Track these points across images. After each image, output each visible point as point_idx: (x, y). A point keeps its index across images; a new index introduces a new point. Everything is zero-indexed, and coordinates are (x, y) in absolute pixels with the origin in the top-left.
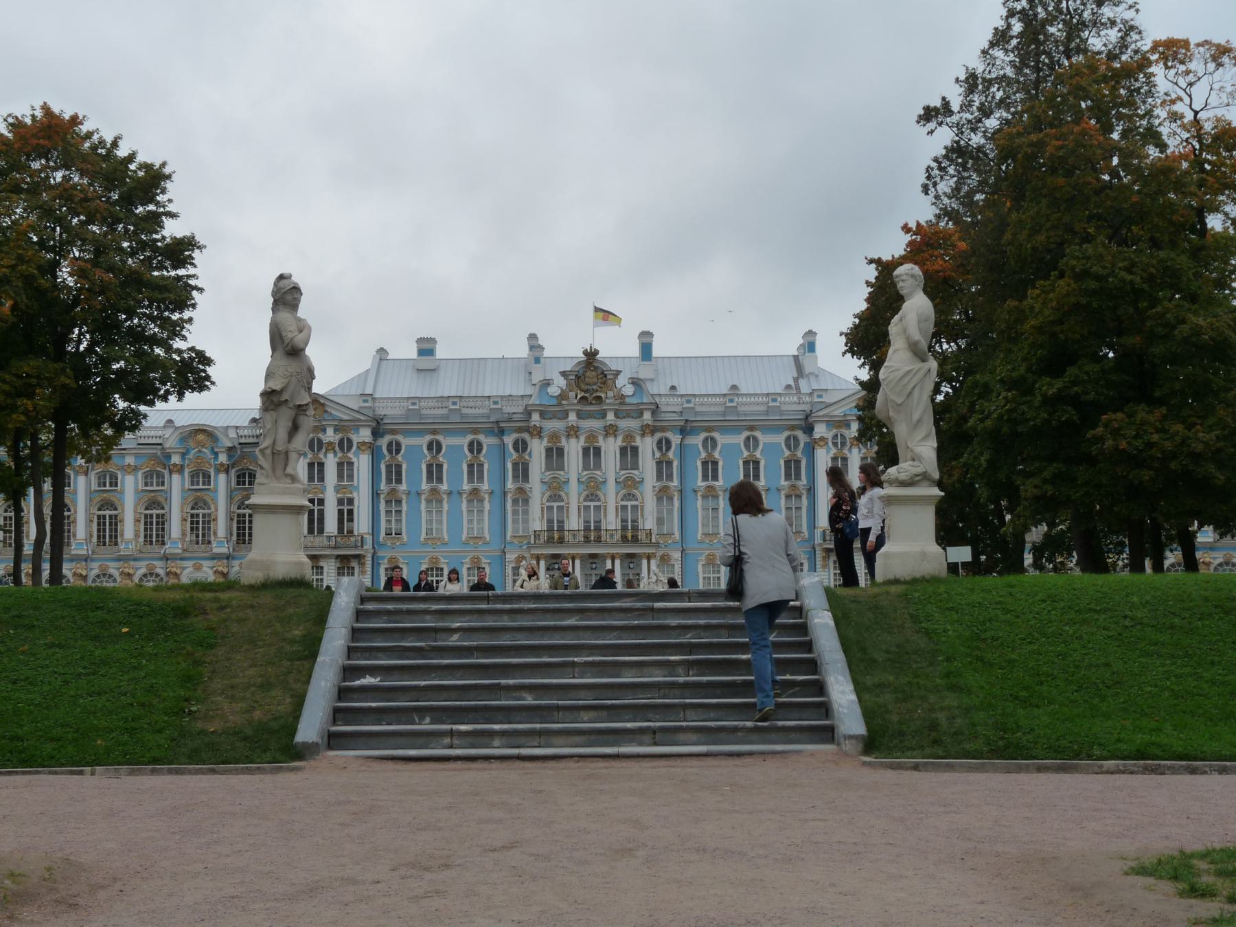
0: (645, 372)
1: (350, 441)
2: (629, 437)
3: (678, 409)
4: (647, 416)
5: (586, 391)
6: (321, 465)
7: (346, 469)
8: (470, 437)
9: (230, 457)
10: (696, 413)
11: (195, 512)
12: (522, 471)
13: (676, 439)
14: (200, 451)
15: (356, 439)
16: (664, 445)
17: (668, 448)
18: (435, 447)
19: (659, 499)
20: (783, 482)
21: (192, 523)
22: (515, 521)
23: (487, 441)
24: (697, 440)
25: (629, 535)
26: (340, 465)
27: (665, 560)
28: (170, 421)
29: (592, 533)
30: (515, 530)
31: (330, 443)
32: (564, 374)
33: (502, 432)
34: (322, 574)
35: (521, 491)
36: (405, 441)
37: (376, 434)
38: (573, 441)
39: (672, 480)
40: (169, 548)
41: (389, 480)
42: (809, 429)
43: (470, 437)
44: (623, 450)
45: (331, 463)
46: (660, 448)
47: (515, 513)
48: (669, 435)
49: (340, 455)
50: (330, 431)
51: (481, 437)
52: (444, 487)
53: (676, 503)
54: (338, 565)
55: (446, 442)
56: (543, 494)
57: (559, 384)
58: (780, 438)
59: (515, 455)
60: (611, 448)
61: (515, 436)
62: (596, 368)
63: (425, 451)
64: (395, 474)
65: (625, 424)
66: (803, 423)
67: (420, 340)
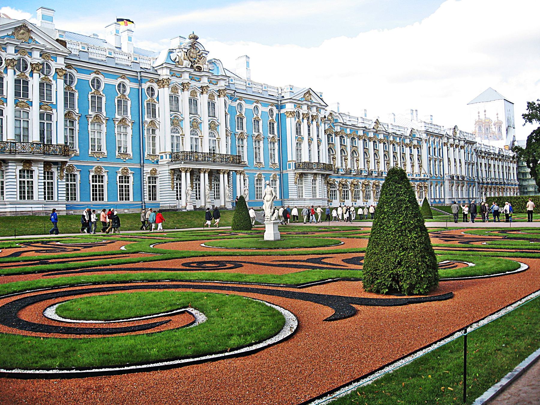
1: (49, 67)
15: (54, 66)
26: (41, 85)
45: (34, 82)
51: (127, 81)
55: (104, 81)
59: (149, 98)
61: (149, 84)
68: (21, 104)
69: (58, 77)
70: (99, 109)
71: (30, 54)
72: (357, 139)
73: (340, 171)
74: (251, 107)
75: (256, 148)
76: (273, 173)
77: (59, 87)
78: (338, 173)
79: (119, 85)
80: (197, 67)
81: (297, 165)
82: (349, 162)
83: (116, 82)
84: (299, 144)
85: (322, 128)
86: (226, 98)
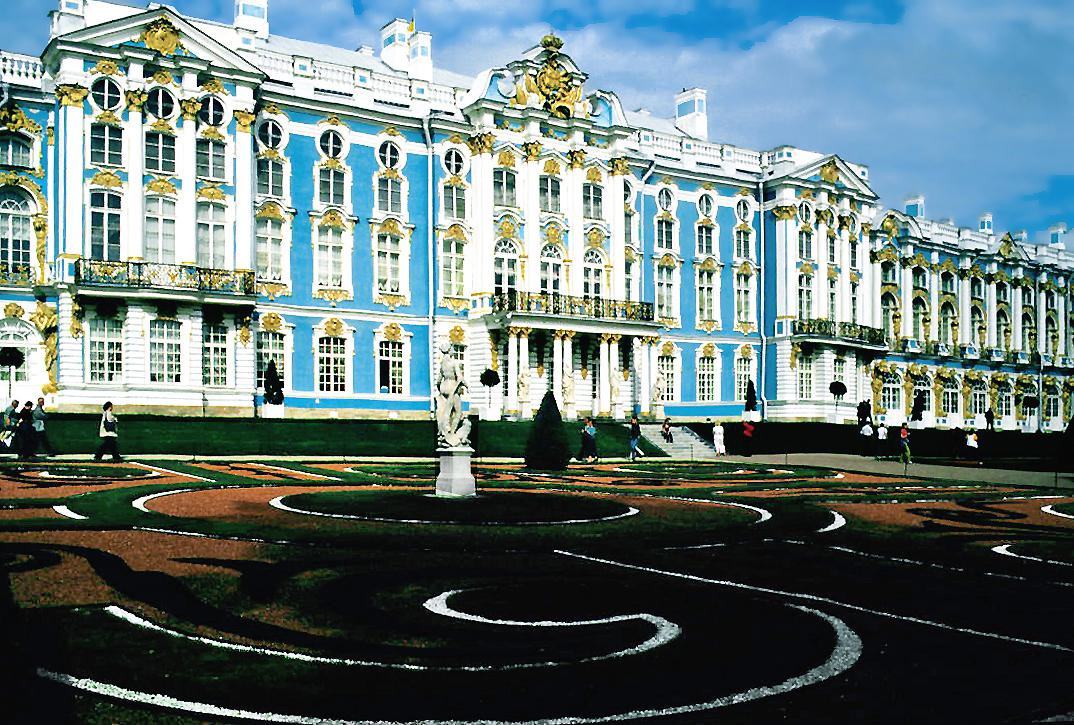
1: (218, 106)
2: (595, 173)
12: (457, 201)
23: (407, 147)
26: (202, 144)
45: (186, 138)
55: (349, 137)
59: (449, 176)
68: (105, 177)
70: (395, 208)
72: (955, 278)
73: (909, 345)
74: (693, 197)
75: (739, 291)
76: (743, 344)
77: (240, 149)
78: (904, 351)
79: (325, 137)
80: (561, 109)
81: (797, 325)
82: (934, 327)
83: (375, 141)
84: (805, 278)
85: (865, 247)
86: (632, 178)
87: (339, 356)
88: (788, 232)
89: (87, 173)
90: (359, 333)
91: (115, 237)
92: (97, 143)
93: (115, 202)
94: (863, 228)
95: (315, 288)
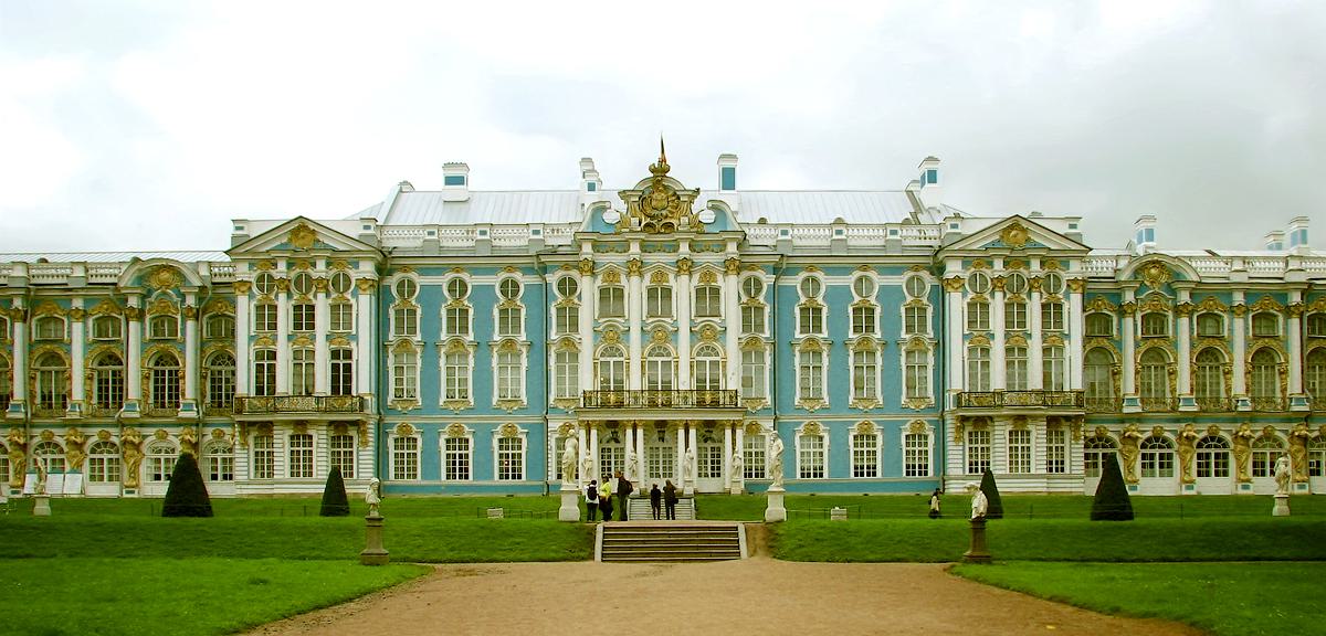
0: (728, 197)
1: (347, 279)
3: (771, 242)
4: (732, 248)
5: (652, 217)
6: (312, 308)
7: (341, 311)
8: (503, 275)
9: (200, 299)
10: (795, 248)
11: (160, 368)
12: (570, 318)
13: (767, 279)
14: (164, 293)
15: (354, 275)
16: (751, 287)
17: (758, 291)
18: (458, 287)
19: (746, 355)
20: (904, 335)
21: (156, 381)
22: (560, 381)
24: (796, 281)
25: (708, 397)
26: (334, 308)
27: (753, 430)
28: (136, 260)
29: (659, 394)
30: (560, 390)
31: (321, 280)
32: (624, 194)
33: (544, 270)
34: (311, 445)
35: (567, 341)
36: (420, 281)
37: (383, 270)
38: (635, 279)
39: (763, 332)
40: (124, 413)
41: (399, 328)
42: (938, 270)
43: (503, 275)
44: (700, 292)
45: (322, 305)
46: (748, 292)
47: (560, 370)
48: (760, 274)
49: (334, 295)
50: (321, 265)
51: (518, 276)
52: (471, 337)
53: (768, 360)
54: (332, 434)
55: (472, 281)
56: (596, 346)
57: (617, 210)
58: (900, 281)
59: (561, 298)
60: (683, 289)
61: (560, 274)
62: (665, 187)
63: (446, 293)
64: (406, 318)
65: (704, 258)
66: (930, 261)
67: (447, 165)
69: (361, 292)
71: (314, 265)
76: (913, 420)
87: (463, 452)
88: (957, 304)
89: (251, 338)
90: (479, 434)
91: (272, 378)
92: (260, 317)
93: (273, 355)
94: (1068, 285)
95: (495, 399)
